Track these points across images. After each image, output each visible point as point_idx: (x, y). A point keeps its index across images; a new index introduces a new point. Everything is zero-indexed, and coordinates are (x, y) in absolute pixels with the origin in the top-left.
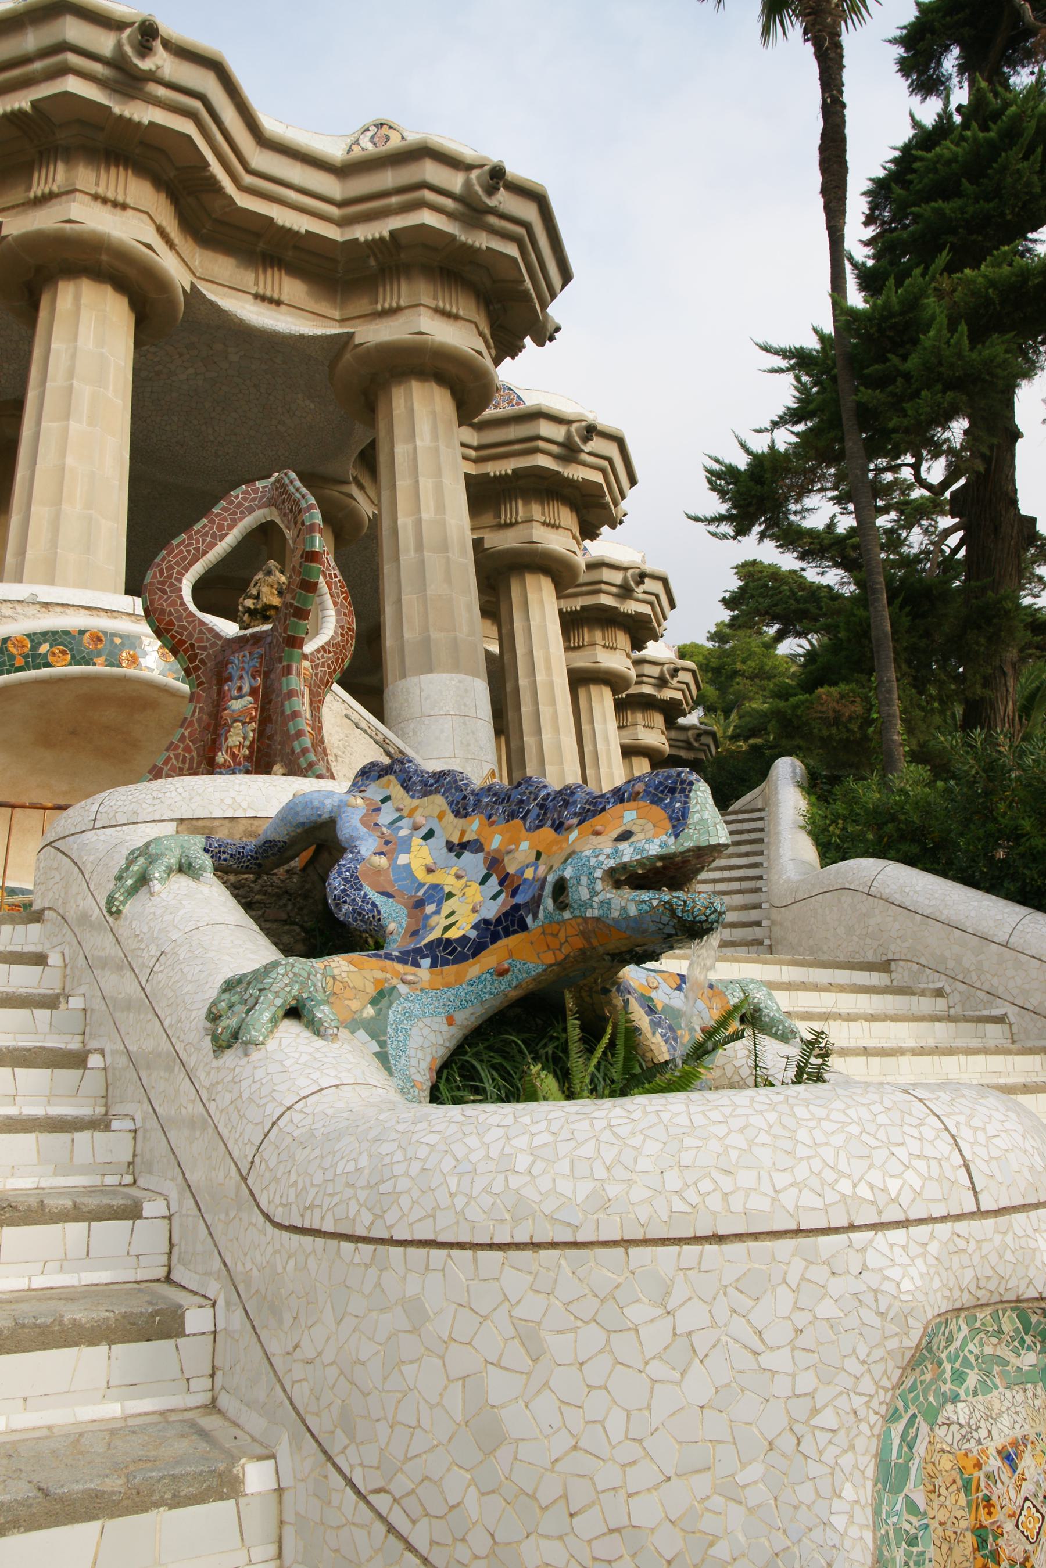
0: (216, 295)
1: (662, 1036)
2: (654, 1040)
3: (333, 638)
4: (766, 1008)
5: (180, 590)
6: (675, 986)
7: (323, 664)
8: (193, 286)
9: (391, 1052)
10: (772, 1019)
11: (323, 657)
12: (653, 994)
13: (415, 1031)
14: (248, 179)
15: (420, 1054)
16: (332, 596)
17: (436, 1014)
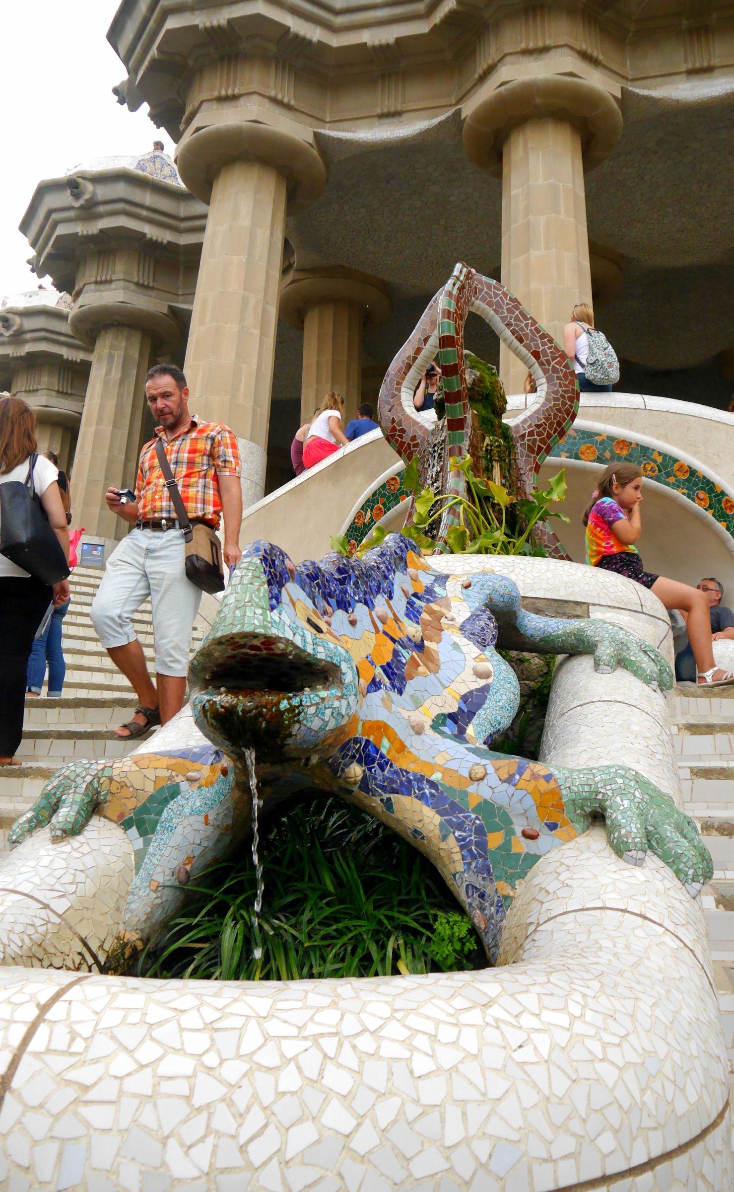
0: (649, 88)
1: (458, 840)
2: (442, 845)
3: (544, 405)
4: (611, 807)
5: (400, 398)
6: (505, 776)
7: (531, 434)
8: (624, 91)
9: (151, 850)
10: (612, 821)
11: (530, 426)
12: (472, 789)
13: (179, 830)
14: (339, 20)
15: (175, 853)
16: (541, 364)
17: (198, 813)
